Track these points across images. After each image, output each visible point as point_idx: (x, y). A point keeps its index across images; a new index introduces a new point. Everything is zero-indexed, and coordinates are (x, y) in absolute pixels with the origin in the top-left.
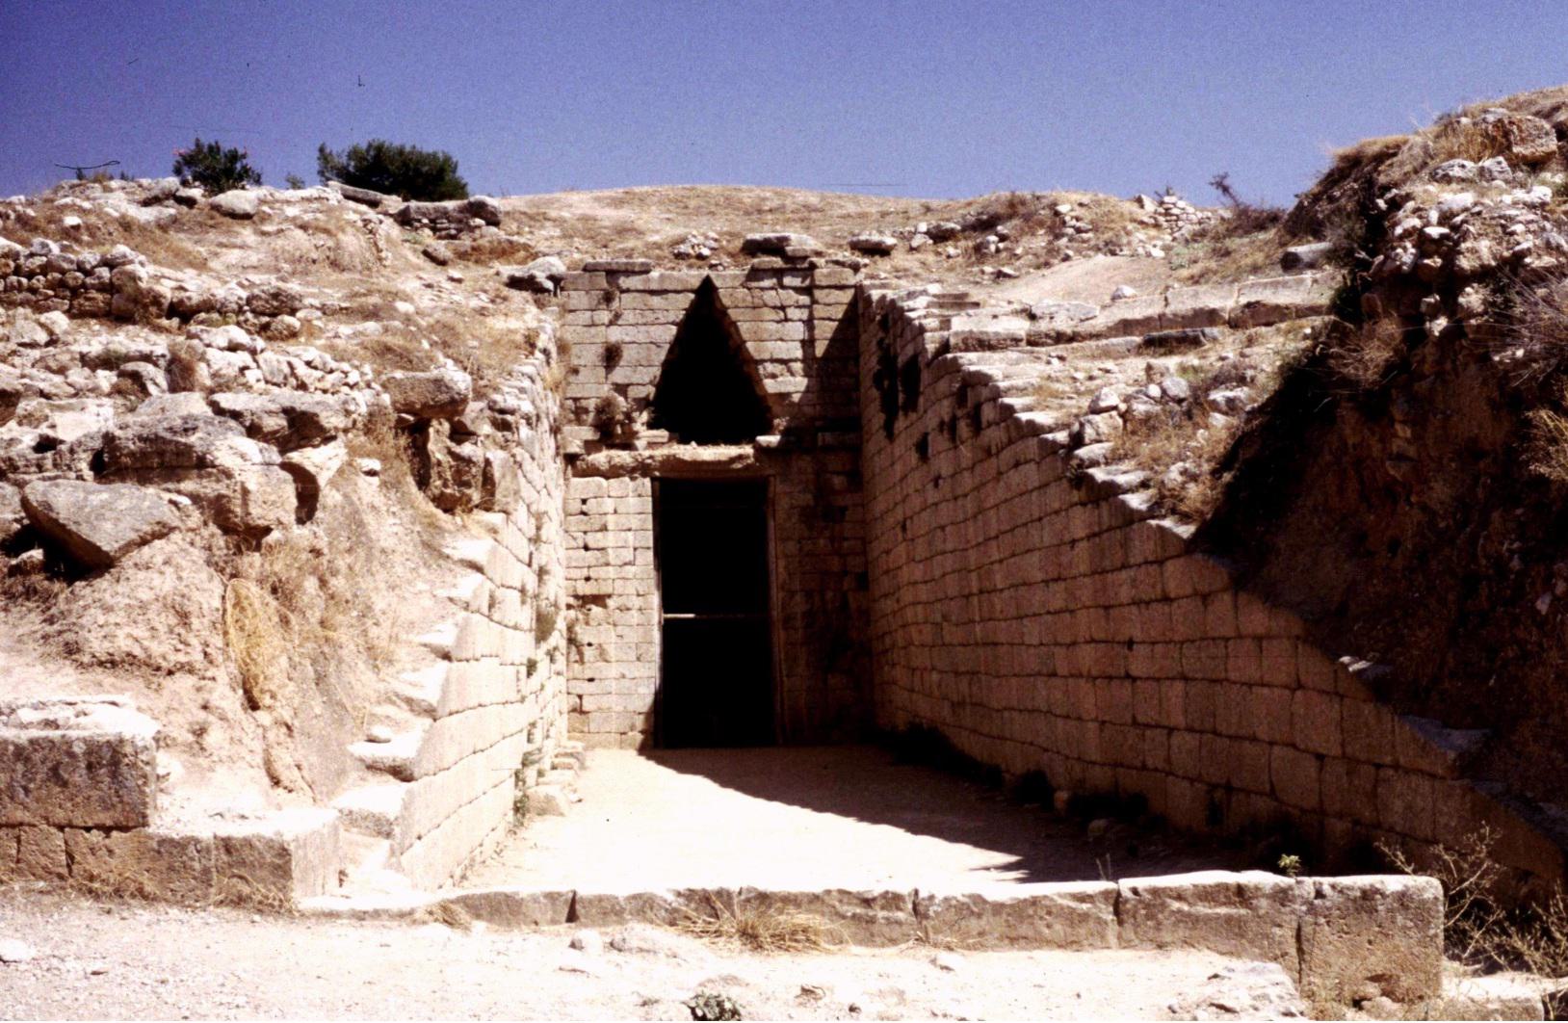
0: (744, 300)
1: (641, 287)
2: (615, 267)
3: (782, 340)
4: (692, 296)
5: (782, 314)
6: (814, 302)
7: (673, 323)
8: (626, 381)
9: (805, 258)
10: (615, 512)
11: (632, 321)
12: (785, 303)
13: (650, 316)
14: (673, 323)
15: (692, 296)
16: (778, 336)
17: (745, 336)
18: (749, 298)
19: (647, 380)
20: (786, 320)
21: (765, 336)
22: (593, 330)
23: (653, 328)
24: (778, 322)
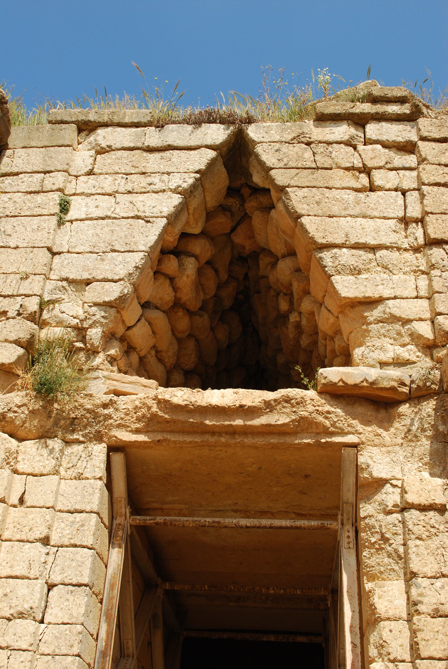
0: (300, 157)
1: (132, 145)
2: (92, 117)
3: (364, 217)
4: (212, 154)
5: (364, 180)
6: (422, 160)
7: (175, 191)
8: (86, 276)
9: (402, 101)
10: (22, 501)
11: (109, 190)
12: (370, 164)
13: (143, 181)
14: (175, 191)
15: (212, 154)
16: (356, 211)
17: (301, 208)
18: (308, 154)
19: (122, 272)
20: (372, 188)
21: (335, 210)
22: (39, 198)
23: (141, 197)
24: (357, 190)
